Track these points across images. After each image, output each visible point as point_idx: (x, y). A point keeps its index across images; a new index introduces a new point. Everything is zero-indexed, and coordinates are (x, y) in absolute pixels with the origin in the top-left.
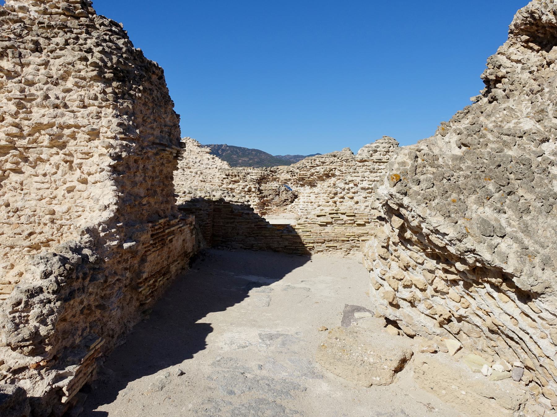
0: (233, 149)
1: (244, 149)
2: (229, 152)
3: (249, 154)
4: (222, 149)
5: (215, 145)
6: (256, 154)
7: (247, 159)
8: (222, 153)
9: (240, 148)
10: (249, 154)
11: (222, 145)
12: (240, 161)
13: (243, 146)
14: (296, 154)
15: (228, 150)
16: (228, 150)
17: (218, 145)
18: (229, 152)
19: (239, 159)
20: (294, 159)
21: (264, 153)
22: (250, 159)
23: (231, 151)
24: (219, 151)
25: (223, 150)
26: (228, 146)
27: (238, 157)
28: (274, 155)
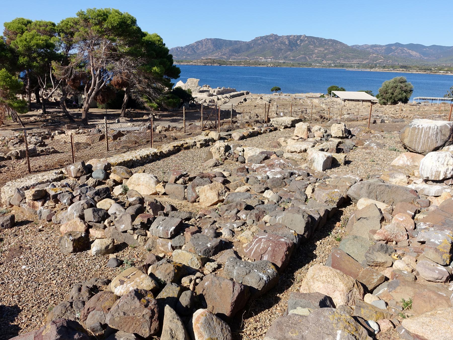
0: (311, 39)
1: (321, 39)
2: (307, 42)
3: (326, 44)
4: (301, 40)
5: (294, 36)
6: (332, 45)
7: (322, 49)
8: (301, 44)
9: (317, 39)
10: (326, 44)
11: (301, 36)
12: (316, 51)
13: (320, 36)
14: (374, 44)
15: (306, 40)
16: (306, 40)
17: (297, 36)
18: (307, 42)
19: (316, 49)
20: (371, 49)
21: (340, 43)
22: (326, 49)
23: (309, 42)
24: (298, 42)
25: (302, 41)
26: (306, 37)
27: (314, 47)
28: (350, 44)
